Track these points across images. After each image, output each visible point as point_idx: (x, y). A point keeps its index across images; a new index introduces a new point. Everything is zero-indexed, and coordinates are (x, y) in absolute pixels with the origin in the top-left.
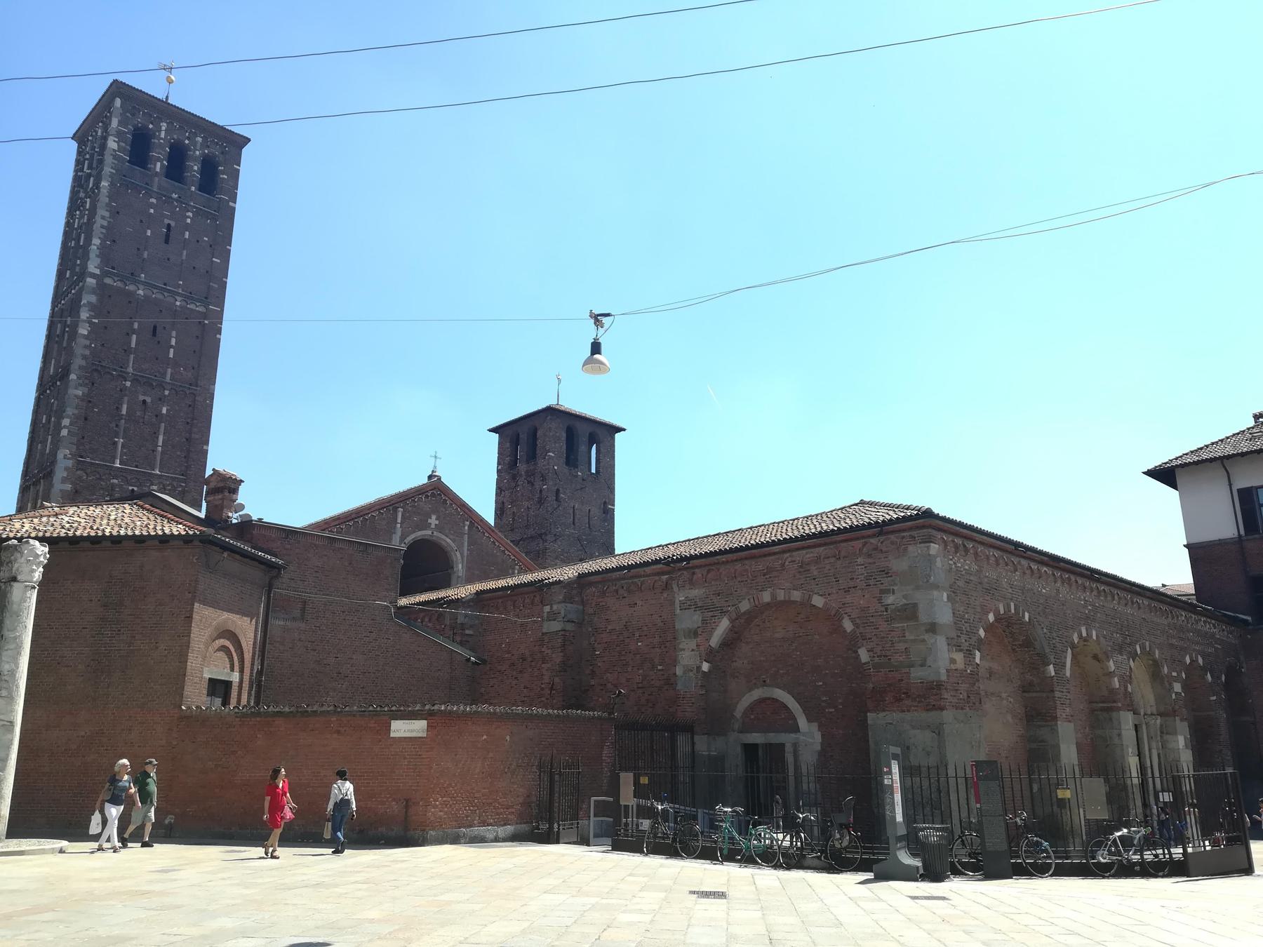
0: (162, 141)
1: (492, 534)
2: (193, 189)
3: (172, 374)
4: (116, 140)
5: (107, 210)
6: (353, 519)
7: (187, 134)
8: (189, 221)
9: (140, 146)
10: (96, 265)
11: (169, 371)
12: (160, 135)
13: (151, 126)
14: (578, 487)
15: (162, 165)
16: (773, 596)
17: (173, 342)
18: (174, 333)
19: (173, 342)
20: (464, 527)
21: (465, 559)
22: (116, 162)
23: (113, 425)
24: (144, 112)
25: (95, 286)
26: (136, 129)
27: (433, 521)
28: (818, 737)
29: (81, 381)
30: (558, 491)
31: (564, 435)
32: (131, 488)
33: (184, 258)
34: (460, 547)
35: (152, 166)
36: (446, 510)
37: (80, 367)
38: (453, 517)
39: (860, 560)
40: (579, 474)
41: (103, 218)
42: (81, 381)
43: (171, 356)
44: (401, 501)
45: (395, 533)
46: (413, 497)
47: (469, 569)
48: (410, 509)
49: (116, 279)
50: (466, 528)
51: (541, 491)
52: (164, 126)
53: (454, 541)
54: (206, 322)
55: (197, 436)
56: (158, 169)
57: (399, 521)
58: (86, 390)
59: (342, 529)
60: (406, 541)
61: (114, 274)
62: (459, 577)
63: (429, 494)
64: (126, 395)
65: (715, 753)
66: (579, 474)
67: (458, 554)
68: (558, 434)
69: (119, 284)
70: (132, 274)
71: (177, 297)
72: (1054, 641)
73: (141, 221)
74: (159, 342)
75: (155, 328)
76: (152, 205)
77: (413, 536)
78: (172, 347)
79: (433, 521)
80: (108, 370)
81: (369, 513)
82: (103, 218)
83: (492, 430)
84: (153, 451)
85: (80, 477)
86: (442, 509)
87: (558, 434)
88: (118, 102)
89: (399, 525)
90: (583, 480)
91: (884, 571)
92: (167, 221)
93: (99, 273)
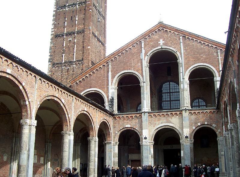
1: (198, 38)
17: (77, 19)
19: (77, 19)
21: (183, 54)
36: (168, 35)
43: (77, 23)
45: (142, 53)
47: (186, 59)
48: (148, 40)
53: (175, 48)
55: (85, 45)
57: (143, 46)
60: (148, 54)
61: (60, 8)
79: (161, 42)
89: (143, 49)
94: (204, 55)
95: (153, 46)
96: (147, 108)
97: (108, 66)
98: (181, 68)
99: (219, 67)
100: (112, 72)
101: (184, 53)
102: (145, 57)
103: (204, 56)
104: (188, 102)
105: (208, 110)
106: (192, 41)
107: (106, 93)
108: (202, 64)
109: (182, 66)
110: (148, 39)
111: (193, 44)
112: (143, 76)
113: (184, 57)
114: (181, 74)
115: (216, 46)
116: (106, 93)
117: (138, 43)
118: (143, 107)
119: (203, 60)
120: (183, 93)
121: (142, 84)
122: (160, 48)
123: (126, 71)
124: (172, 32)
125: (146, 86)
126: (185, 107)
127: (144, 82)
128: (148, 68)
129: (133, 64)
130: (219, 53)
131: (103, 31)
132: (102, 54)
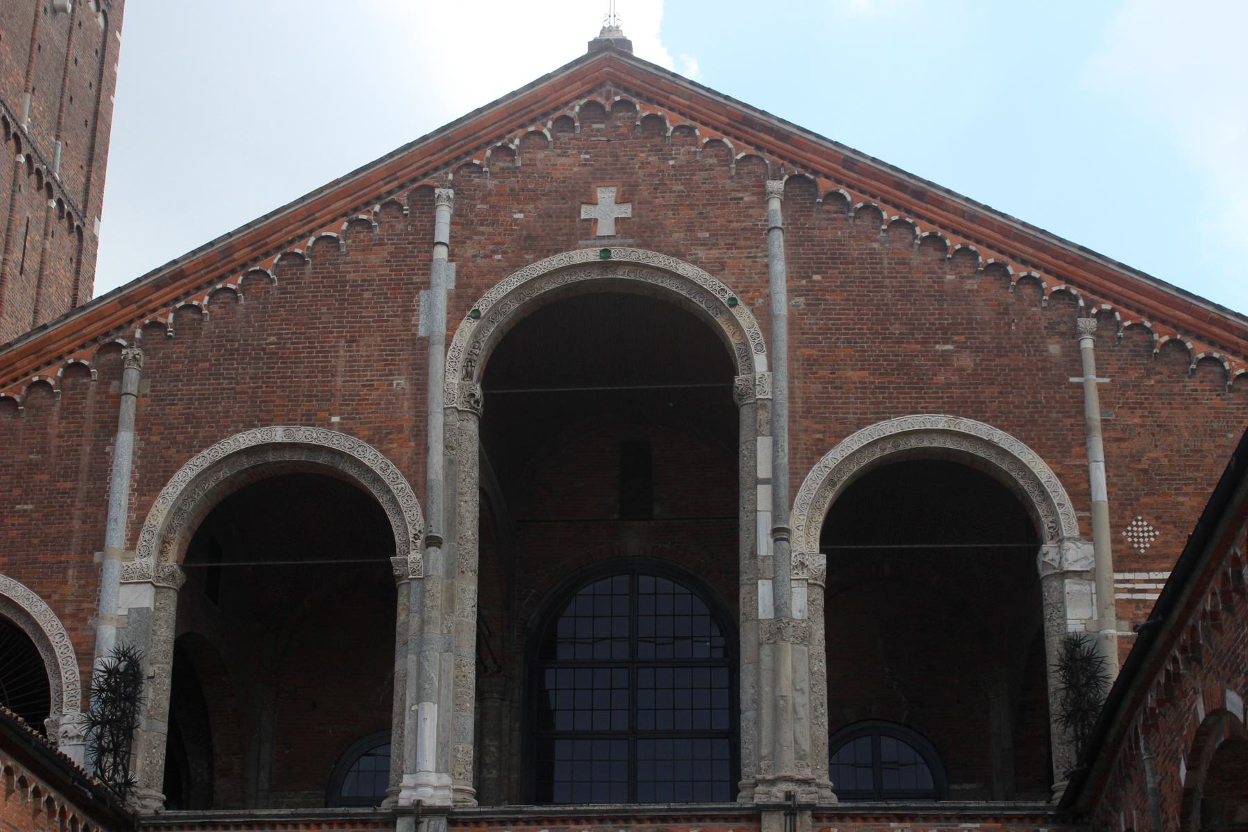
1: (919, 205)
6: (244, 266)
36: (664, 159)
38: (700, 176)
44: (447, 164)
45: (427, 285)
46: (500, 137)
48: (491, 184)
50: (775, 205)
53: (717, 268)
57: (443, 232)
59: (198, 309)
60: (483, 306)
62: (758, 406)
63: (572, 114)
67: (744, 316)
77: (513, 281)
81: (311, 232)
89: (441, 253)
94: (961, 347)
95: (528, 237)
96: (446, 779)
97: (117, 371)
98: (763, 445)
99: (1085, 456)
100: (142, 427)
101: (792, 323)
102: (452, 328)
103: (966, 361)
104: (814, 743)
105: (984, 819)
106: (867, 221)
107: (73, 616)
108: (941, 421)
109: (771, 422)
110: (494, 175)
111: (872, 253)
112: (421, 488)
113: (792, 349)
114: (764, 493)
115: (1068, 281)
116: (73, 616)
117: (402, 197)
118: (408, 763)
119: (949, 385)
120: (776, 659)
121: (410, 558)
122: (592, 255)
123: (278, 434)
124: (703, 135)
125: (450, 574)
126: (785, 787)
127: (432, 541)
128: (472, 427)
129: (339, 380)
130: (1088, 343)
131: (79, 113)
132: (61, 271)
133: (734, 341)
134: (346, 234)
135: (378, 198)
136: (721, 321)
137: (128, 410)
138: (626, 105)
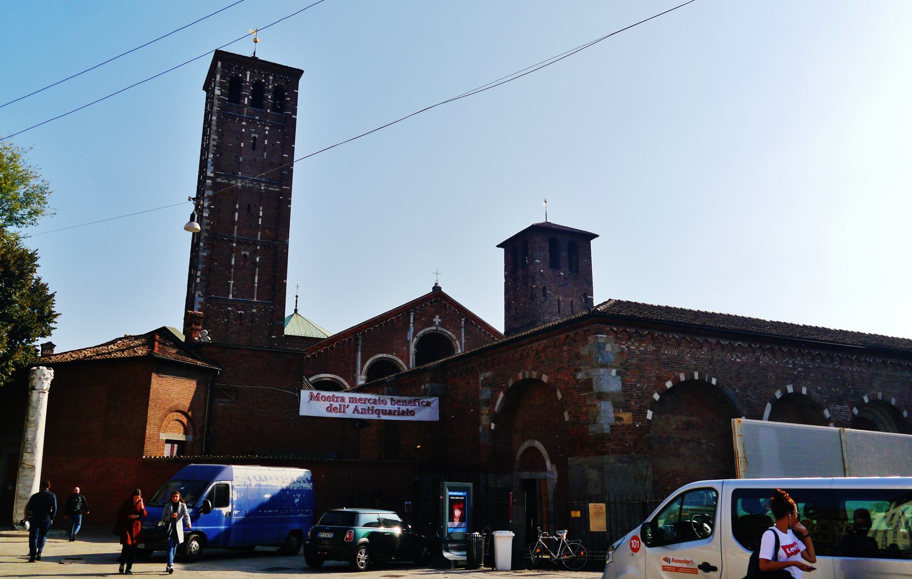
0: (248, 84)
2: (269, 111)
3: (261, 235)
4: (220, 88)
5: (216, 135)
7: (263, 76)
8: (267, 132)
9: (234, 89)
10: (211, 171)
11: (259, 233)
12: (246, 79)
13: (240, 75)
14: (561, 284)
15: (249, 99)
16: (524, 375)
17: (261, 213)
18: (261, 208)
19: (261, 213)
20: (461, 322)
22: (220, 103)
23: (226, 272)
24: (235, 67)
25: (211, 185)
26: (231, 78)
27: (437, 320)
28: (556, 476)
29: (206, 247)
30: (544, 289)
31: (548, 245)
32: (239, 312)
33: (265, 157)
34: (459, 337)
35: (243, 101)
37: (205, 237)
39: (565, 348)
40: (562, 274)
41: (214, 140)
42: (206, 247)
43: (260, 223)
45: (409, 330)
49: (223, 178)
50: (463, 323)
51: (532, 290)
52: (248, 73)
53: (453, 333)
54: (281, 198)
56: (246, 102)
57: (412, 321)
58: (209, 252)
59: (371, 330)
60: (418, 335)
64: (233, 253)
65: (501, 486)
66: (562, 274)
67: (457, 342)
68: (542, 245)
69: (226, 181)
70: (234, 173)
71: (262, 184)
72: (749, 398)
73: (237, 138)
74: (252, 215)
75: (249, 206)
76: (243, 127)
78: (260, 217)
79: (437, 320)
80: (221, 238)
81: (390, 318)
82: (214, 140)
83: (498, 246)
84: (253, 286)
85: (209, 308)
86: (443, 310)
87: (542, 245)
88: (219, 64)
89: (411, 325)
90: (565, 278)
91: (576, 355)
92: (253, 135)
93: (213, 176)
97: (357, 340)
100: (362, 352)
122: (434, 328)
123: (385, 355)
129: (395, 346)
133: (455, 346)
134: (396, 319)
135: (401, 313)
136: (453, 342)
137: (360, 348)
138: (441, 300)
